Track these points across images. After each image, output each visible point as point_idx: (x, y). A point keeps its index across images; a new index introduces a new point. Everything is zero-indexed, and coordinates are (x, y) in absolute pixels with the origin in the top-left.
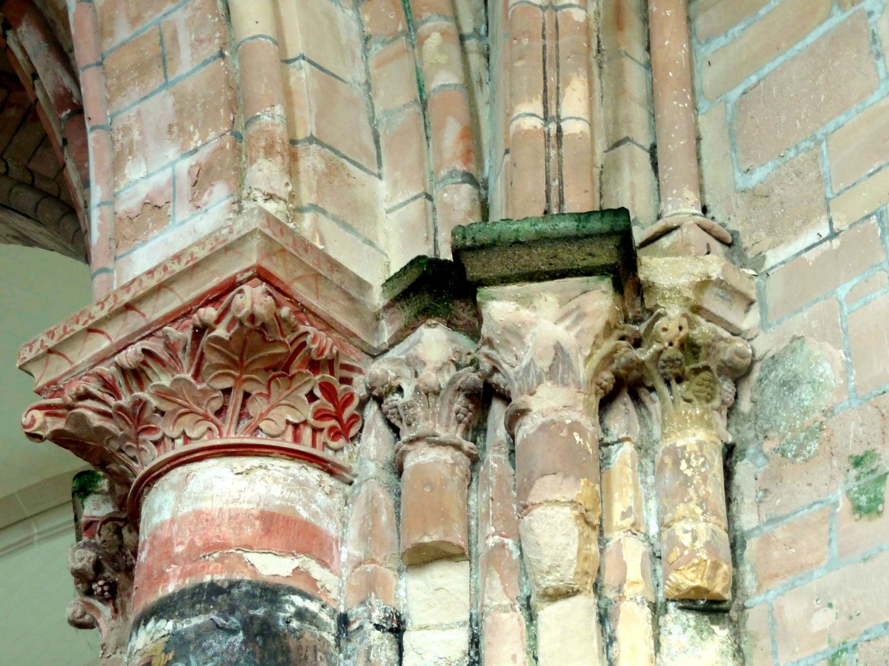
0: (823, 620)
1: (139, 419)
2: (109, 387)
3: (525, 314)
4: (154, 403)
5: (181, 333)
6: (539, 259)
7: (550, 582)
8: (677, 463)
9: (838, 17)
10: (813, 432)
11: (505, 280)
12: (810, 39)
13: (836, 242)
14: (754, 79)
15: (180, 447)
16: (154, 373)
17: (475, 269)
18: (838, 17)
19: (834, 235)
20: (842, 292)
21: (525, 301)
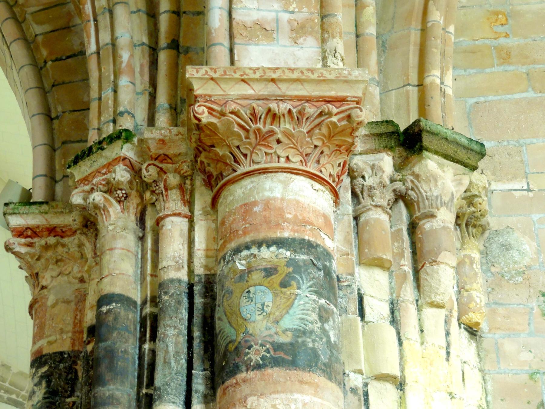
0: (525, 356)
1: (265, 139)
2: (254, 117)
3: (439, 172)
4: (280, 136)
5: (311, 110)
6: (450, 149)
7: (438, 299)
8: (472, 263)
9: (531, 94)
10: (518, 273)
11: (436, 153)
12: (517, 96)
13: (531, 194)
14: (482, 99)
15: (283, 163)
16: (285, 121)
17: (427, 140)
19: (529, 190)
20: (536, 217)
21: (441, 166)
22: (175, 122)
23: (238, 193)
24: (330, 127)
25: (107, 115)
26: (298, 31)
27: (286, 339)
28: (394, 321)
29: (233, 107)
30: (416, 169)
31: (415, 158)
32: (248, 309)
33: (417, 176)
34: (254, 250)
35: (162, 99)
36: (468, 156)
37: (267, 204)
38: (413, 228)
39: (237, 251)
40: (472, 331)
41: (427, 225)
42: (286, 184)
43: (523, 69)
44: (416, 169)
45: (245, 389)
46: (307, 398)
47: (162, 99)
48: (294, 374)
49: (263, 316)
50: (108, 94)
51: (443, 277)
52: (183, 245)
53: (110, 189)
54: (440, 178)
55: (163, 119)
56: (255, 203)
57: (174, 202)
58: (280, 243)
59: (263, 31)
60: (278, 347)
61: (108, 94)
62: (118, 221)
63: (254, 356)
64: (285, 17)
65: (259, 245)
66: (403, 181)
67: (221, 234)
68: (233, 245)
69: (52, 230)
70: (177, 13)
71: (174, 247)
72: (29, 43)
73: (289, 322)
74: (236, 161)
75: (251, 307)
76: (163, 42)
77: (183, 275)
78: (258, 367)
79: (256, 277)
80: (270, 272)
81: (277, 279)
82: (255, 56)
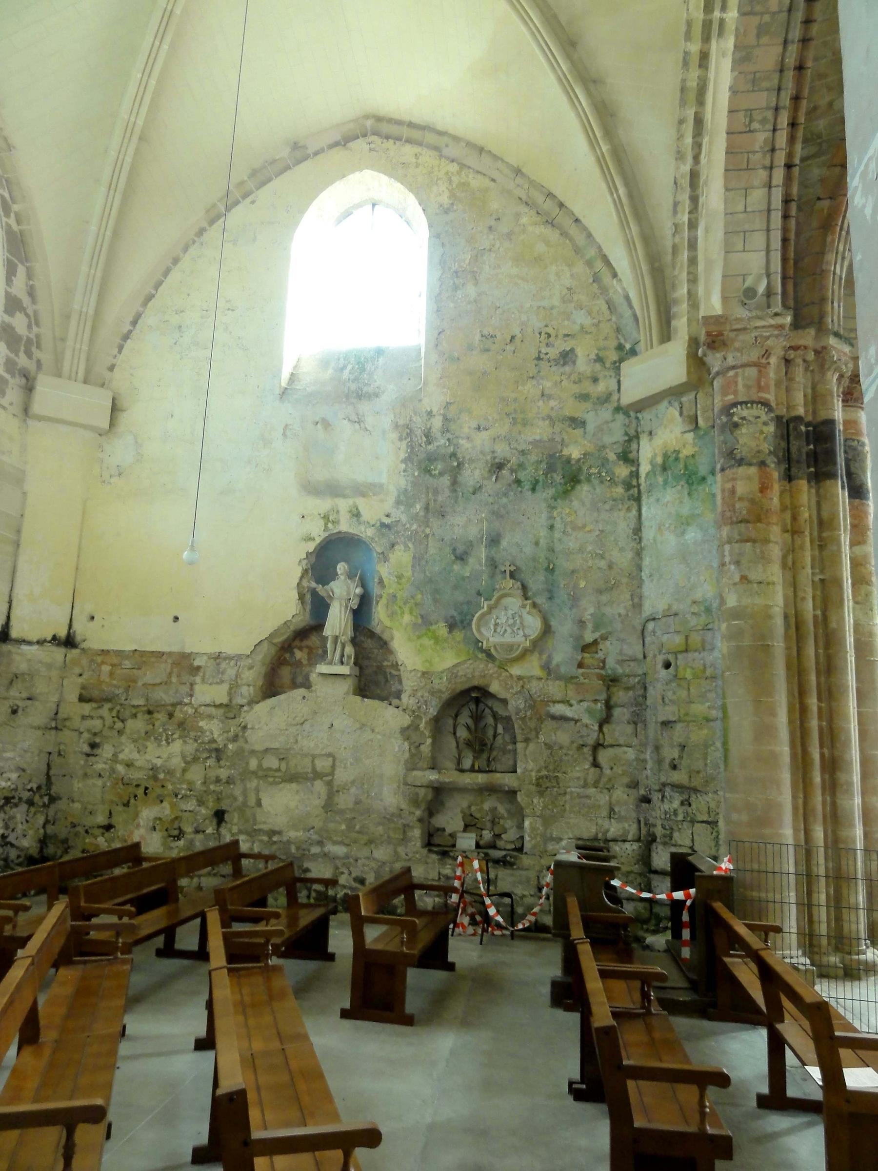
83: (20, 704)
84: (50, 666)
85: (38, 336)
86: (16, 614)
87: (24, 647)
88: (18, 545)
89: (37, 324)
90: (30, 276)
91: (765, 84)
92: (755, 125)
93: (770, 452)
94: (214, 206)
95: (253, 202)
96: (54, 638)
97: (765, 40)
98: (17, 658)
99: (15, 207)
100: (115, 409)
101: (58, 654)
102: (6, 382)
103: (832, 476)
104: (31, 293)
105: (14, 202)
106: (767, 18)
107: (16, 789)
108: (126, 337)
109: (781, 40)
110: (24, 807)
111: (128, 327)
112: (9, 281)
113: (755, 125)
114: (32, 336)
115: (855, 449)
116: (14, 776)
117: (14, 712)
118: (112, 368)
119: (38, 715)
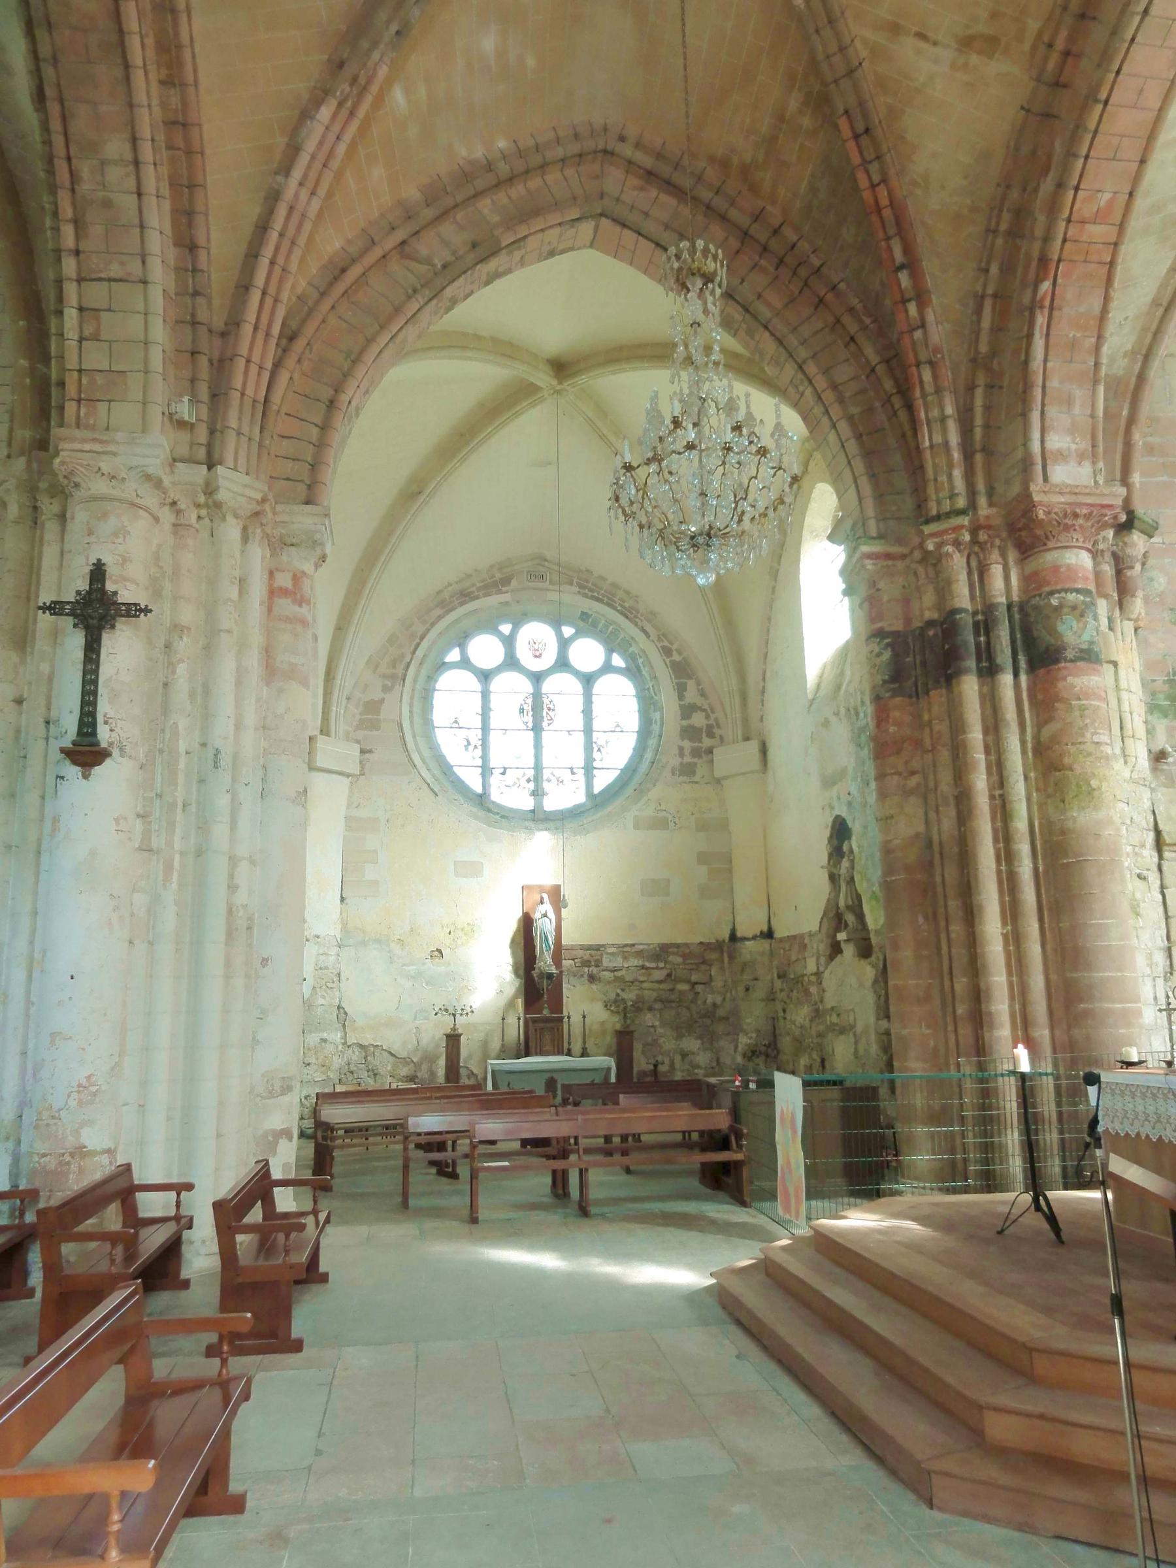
0: (1161, 645)
2: (1065, 515)
9: (1165, 478)
18: (1165, 478)
20: (1167, 561)
22: (991, 505)
23: (1050, 557)
24: (1097, 516)
25: (945, 493)
26: (1081, 457)
27: (1085, 646)
28: (1111, 629)
29: (1056, 510)
30: (1126, 539)
31: (1125, 532)
32: (1061, 628)
33: (1125, 544)
34: (1063, 594)
35: (981, 486)
36: (1150, 531)
37: (1069, 567)
38: (1119, 572)
39: (1051, 593)
40: (1136, 630)
41: (1129, 573)
42: (1077, 555)
43: (1161, 460)
44: (1126, 539)
45: (1065, 672)
46: (1096, 678)
47: (981, 486)
48: (1091, 665)
49: (1071, 632)
50: (943, 478)
51: (1138, 606)
52: (1004, 582)
53: (957, 544)
54: (1137, 542)
55: (982, 501)
56: (1060, 566)
57: (995, 555)
58: (1078, 591)
59: (1061, 456)
60: (1082, 651)
61: (943, 478)
62: (957, 563)
63: (1070, 654)
64: (1074, 447)
65: (1066, 591)
66: (1117, 545)
67: (1032, 581)
68: (1047, 589)
69: (888, 556)
70: (987, 426)
71: (997, 583)
72: (850, 418)
73: (1086, 637)
74: (1047, 538)
75: (1064, 627)
76: (978, 446)
77: (1003, 600)
78: (1071, 661)
79: (1065, 610)
80: (1074, 608)
81: (1077, 612)
82: (1060, 474)
83: (751, 983)
84: (763, 954)
85: (716, 720)
86: (738, 919)
87: (747, 943)
88: (730, 871)
89: (713, 712)
90: (698, 683)
91: (782, 359)
92: (801, 388)
93: (885, 682)
94: (771, 567)
95: (522, 710)
96: (762, 932)
97: (757, 337)
98: (744, 951)
99: (674, 647)
100: (764, 750)
101: (765, 945)
102: (695, 764)
103: (959, 672)
104: (703, 694)
105: (672, 644)
106: (744, 326)
107: (756, 1045)
108: (763, 692)
109: (762, 329)
110: (763, 1058)
111: (762, 684)
112: (681, 697)
113: (801, 388)
114: (712, 722)
115: (1036, 608)
116: (754, 1035)
117: (747, 990)
118: (761, 720)
119: (759, 992)
